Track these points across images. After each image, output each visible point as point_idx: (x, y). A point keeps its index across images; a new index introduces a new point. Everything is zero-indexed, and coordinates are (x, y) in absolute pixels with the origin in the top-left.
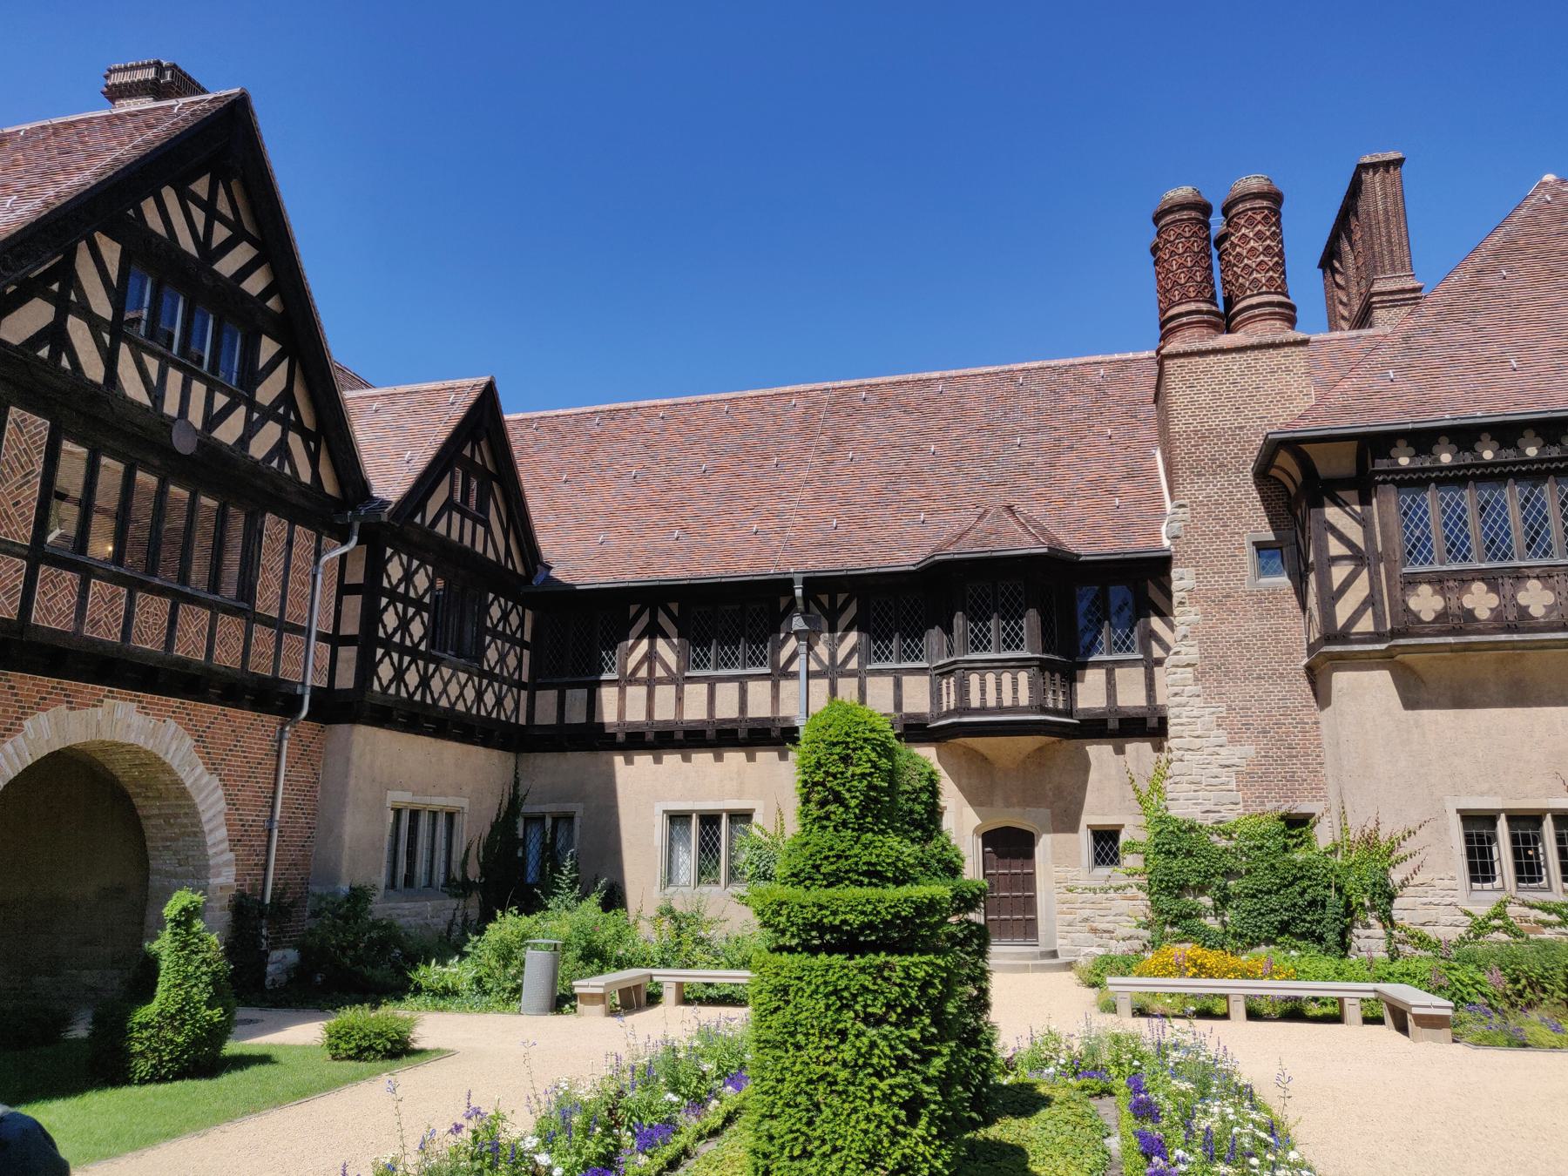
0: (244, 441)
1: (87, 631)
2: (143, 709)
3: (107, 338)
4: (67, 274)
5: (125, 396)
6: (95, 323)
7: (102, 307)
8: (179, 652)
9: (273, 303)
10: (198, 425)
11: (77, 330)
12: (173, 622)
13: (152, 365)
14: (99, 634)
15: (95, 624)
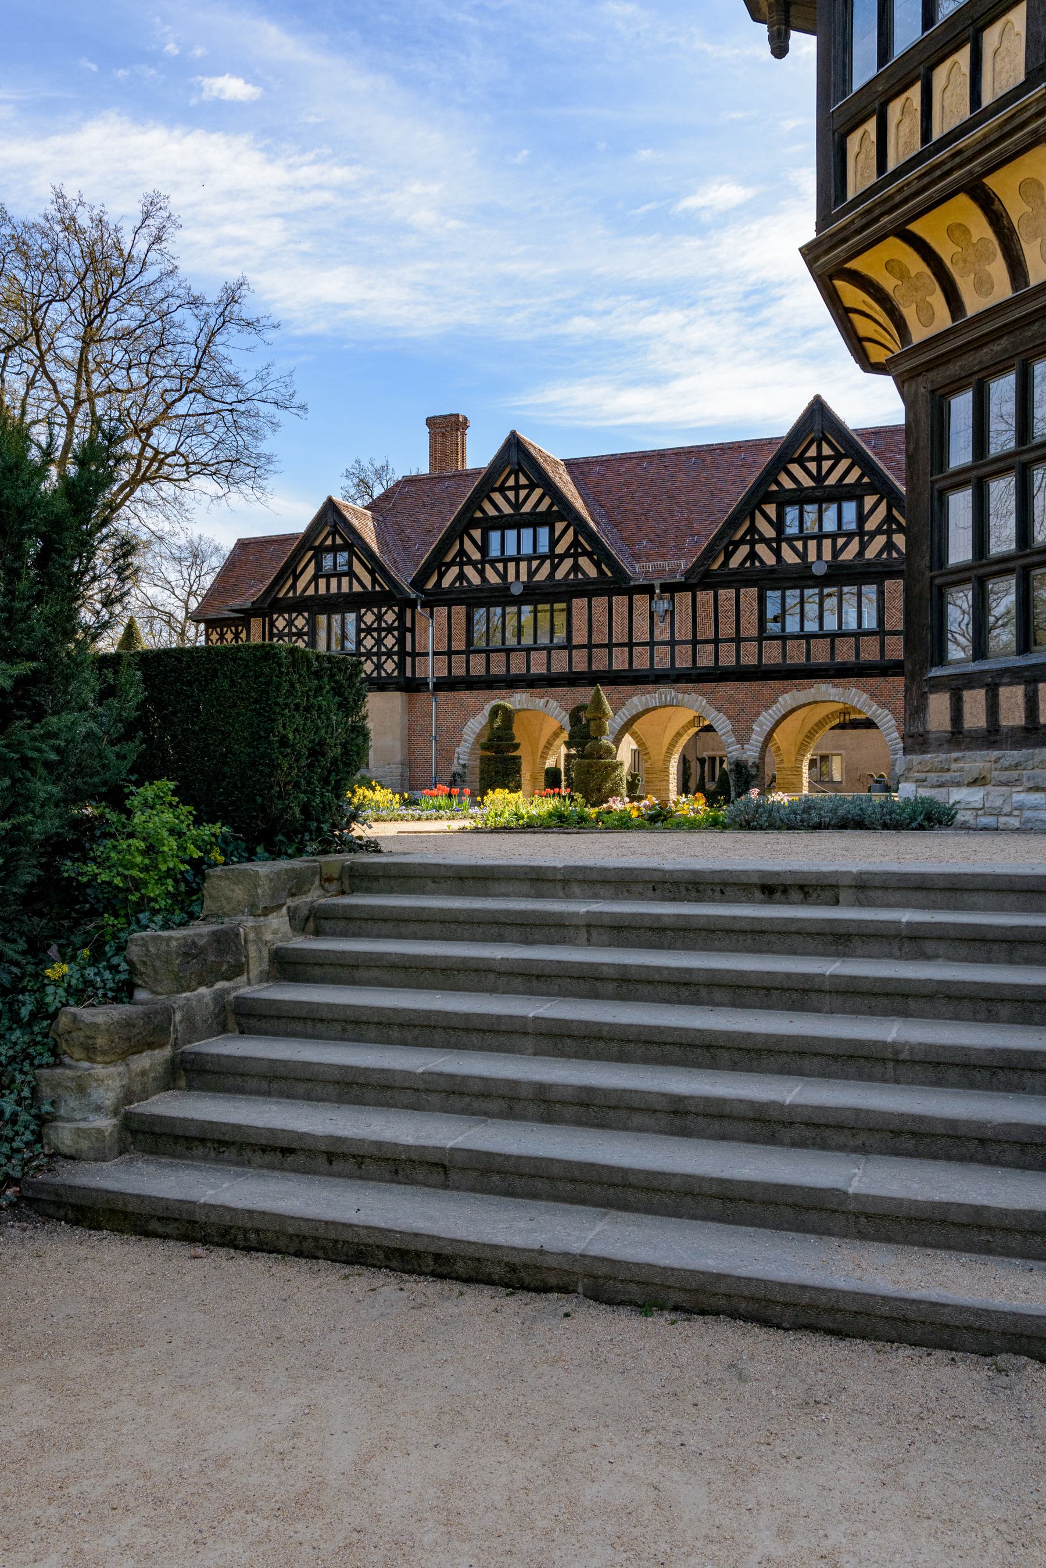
0: (861, 553)
1: (788, 662)
2: (835, 686)
3: (774, 545)
4: (753, 529)
5: (788, 564)
6: (767, 542)
7: (769, 532)
8: (838, 659)
9: (866, 480)
10: (829, 558)
11: (761, 549)
12: (833, 648)
13: (799, 545)
14: (796, 661)
15: (791, 658)
